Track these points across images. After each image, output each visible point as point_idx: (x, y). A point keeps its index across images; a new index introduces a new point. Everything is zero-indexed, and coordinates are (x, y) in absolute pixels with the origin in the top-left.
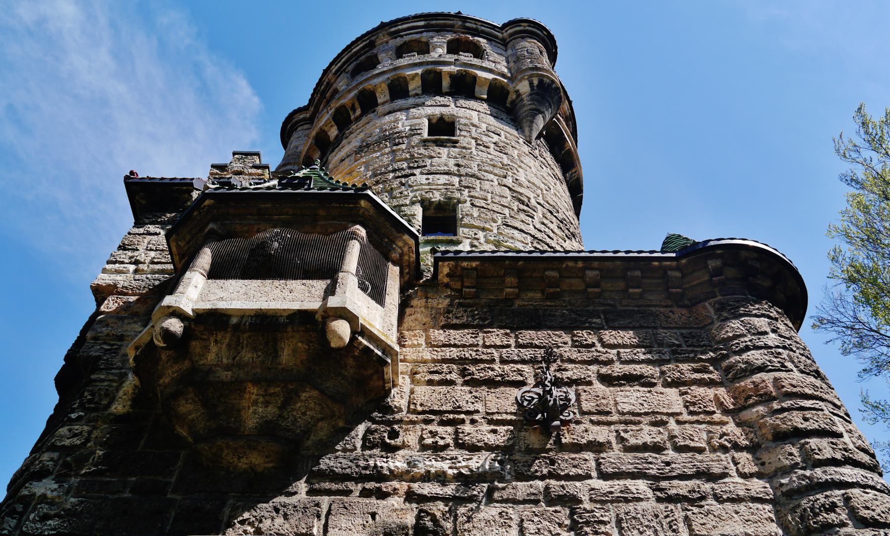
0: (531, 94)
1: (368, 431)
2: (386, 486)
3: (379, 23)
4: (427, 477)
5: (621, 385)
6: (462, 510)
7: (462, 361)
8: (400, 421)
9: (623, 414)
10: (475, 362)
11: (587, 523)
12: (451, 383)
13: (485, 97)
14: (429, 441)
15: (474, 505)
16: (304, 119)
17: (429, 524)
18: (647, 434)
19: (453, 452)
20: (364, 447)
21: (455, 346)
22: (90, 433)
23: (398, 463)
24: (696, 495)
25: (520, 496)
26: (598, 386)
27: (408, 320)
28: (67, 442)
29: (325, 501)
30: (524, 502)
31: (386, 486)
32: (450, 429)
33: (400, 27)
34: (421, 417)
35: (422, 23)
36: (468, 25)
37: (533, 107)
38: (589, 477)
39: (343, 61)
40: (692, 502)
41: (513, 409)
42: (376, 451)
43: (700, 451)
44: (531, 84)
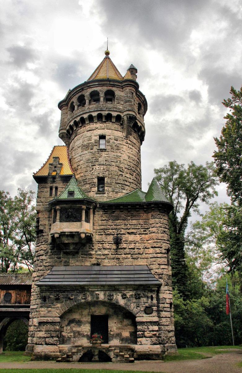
0: (127, 121)
5: (131, 235)
11: (120, 263)
12: (102, 235)
14: (98, 248)
16: (65, 104)
18: (132, 246)
21: (103, 225)
22: (47, 247)
24: (137, 258)
25: (112, 258)
33: (90, 84)
34: (97, 242)
35: (97, 83)
36: (111, 83)
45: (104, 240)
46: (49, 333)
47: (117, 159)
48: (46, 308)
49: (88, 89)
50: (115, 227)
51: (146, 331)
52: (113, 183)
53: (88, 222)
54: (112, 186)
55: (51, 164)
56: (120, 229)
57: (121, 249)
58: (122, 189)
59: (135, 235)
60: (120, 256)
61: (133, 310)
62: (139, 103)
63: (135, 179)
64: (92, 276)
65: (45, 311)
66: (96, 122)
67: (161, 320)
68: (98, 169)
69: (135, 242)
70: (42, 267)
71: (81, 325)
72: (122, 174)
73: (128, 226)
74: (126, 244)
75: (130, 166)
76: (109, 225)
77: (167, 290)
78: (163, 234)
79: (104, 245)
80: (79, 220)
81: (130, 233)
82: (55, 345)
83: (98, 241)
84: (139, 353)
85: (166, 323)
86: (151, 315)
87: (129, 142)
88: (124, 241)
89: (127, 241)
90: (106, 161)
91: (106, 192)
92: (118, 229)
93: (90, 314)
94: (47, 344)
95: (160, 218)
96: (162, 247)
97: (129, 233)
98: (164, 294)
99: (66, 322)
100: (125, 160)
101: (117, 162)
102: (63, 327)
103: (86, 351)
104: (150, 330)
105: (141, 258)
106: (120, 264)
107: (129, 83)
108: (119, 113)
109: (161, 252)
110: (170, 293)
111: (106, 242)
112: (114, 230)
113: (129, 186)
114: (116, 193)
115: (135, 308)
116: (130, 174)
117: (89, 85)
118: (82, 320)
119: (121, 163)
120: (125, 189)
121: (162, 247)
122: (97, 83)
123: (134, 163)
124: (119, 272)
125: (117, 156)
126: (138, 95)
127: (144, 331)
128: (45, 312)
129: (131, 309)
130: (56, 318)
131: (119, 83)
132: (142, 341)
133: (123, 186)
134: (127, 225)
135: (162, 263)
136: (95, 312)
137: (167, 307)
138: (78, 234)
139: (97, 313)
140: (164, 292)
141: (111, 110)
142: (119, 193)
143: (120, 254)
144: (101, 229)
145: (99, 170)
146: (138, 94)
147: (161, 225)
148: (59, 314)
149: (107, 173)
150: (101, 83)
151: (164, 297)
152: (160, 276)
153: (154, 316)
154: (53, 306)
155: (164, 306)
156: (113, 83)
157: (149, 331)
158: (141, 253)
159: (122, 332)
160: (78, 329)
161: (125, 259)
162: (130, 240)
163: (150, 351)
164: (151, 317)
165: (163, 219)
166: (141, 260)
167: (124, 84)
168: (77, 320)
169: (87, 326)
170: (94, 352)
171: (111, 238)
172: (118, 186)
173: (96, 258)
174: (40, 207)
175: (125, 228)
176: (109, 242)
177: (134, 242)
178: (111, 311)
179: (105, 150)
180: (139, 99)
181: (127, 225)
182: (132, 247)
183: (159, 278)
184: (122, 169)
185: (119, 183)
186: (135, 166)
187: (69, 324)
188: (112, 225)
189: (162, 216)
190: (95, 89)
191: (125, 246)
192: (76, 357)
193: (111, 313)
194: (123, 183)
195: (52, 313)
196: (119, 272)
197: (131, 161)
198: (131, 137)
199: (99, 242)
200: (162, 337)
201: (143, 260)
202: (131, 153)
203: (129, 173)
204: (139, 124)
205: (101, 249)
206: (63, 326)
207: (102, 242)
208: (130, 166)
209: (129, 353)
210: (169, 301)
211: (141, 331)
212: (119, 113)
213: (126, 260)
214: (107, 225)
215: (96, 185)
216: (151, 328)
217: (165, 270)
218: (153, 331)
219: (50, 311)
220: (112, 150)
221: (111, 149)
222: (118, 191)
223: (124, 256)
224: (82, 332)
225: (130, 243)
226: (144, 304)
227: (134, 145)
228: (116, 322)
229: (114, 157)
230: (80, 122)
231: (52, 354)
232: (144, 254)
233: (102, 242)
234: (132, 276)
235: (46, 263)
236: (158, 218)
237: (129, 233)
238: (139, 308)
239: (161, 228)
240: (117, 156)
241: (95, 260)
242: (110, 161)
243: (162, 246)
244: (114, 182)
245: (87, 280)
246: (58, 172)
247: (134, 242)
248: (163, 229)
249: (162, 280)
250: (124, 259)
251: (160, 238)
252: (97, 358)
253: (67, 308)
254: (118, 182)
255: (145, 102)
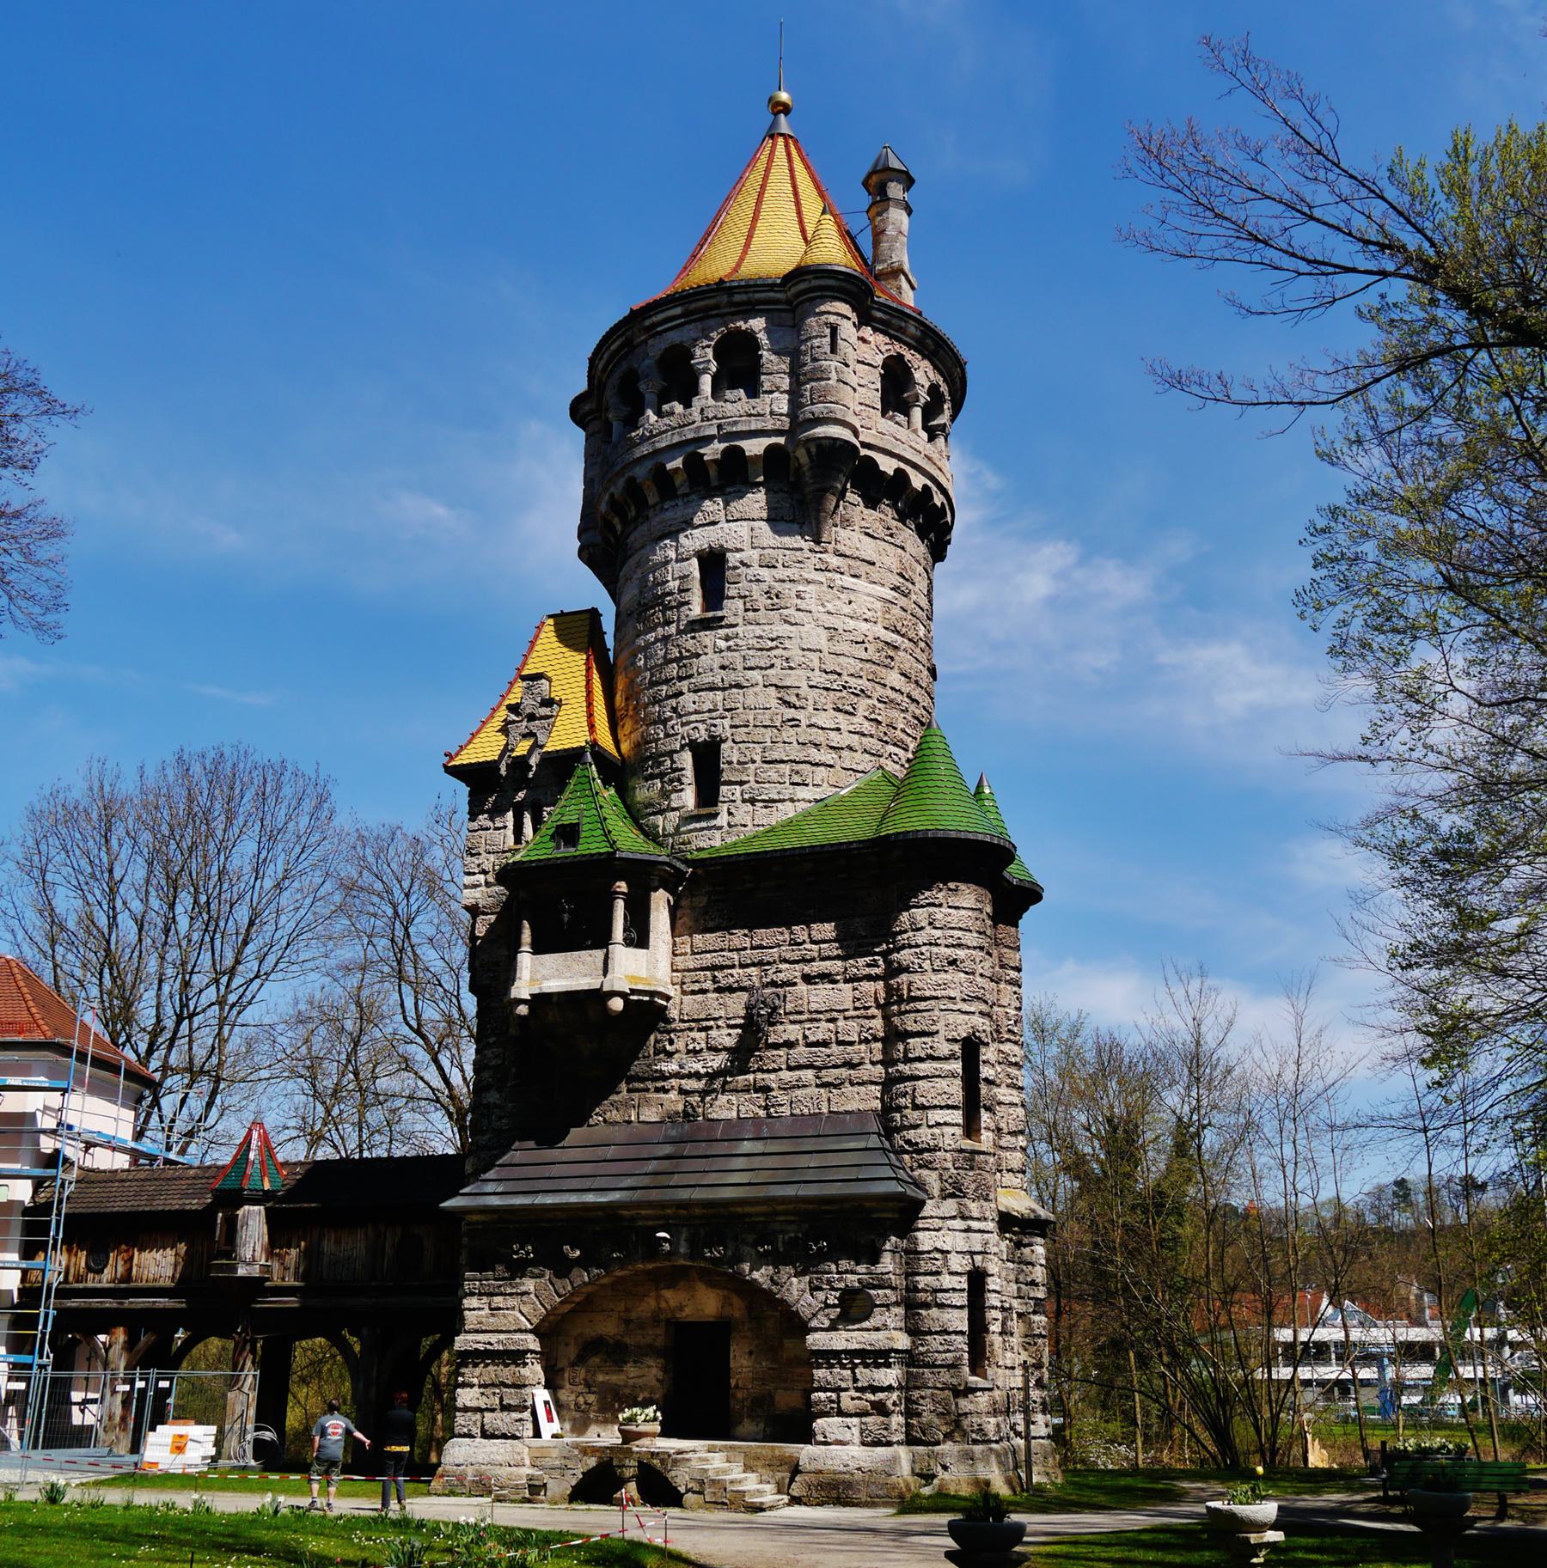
1: (657, 1041)
2: (666, 1084)
3: (627, 312)
4: (690, 1076)
5: (816, 983)
6: (708, 1099)
7: (714, 968)
8: (675, 1030)
9: (811, 1013)
10: (722, 968)
11: (773, 1106)
13: (761, 479)
14: (691, 1047)
15: (714, 1096)
16: (591, 412)
17: (690, 1110)
18: (821, 1031)
19: (706, 1055)
20: (655, 1054)
21: (710, 952)
23: (672, 1067)
25: (740, 1087)
26: (802, 987)
27: (679, 923)
28: (494, 1063)
29: (636, 1096)
30: (742, 1091)
31: (666, 1084)
32: (703, 1034)
33: (654, 319)
34: (687, 1025)
35: (678, 311)
36: (737, 298)
37: (817, 486)
38: (781, 1069)
39: (605, 356)
40: (836, 1086)
41: (742, 1013)
42: (662, 1056)
43: (851, 1043)
44: (809, 452)
45: (712, 1011)
46: (494, 1394)
47: (774, 652)
48: (485, 1299)
49: (650, 342)
50: (756, 955)
51: (846, 1390)
52: (754, 762)
53: (643, 948)
54: (746, 779)
55: (514, 709)
56: (775, 962)
57: (776, 1046)
58: (793, 784)
59: (831, 986)
60: (772, 1076)
61: (798, 1301)
62: (886, 364)
63: (867, 727)
64: (652, 1166)
65: (479, 1309)
66: (687, 495)
67: (922, 1345)
68: (692, 708)
69: (835, 1014)
70: (486, 1137)
71: (625, 1363)
72: (793, 720)
73: (808, 946)
74: (797, 1026)
75: (840, 674)
76: (730, 951)
77: (954, 1218)
78: (943, 975)
79: (713, 1033)
80: (601, 940)
81: (815, 977)
82: (514, 1437)
83: (688, 1021)
84: (813, 1478)
85: (944, 1355)
86: (866, 1324)
87: (835, 561)
88: (791, 1013)
89: (801, 1013)
90: (723, 667)
91: (723, 808)
92: (769, 963)
93: (663, 1317)
94: (485, 1435)
95: (933, 905)
96: (937, 1032)
97: (808, 979)
98: (939, 1234)
99: (572, 1352)
100: (809, 650)
101: (772, 666)
102: (562, 1370)
103: (592, 1462)
104: (860, 1385)
105: (852, 1084)
106: (772, 1110)
107: (815, 283)
108: (774, 440)
109: (929, 1051)
110: (968, 1230)
111: (720, 1023)
112: (749, 970)
113: (831, 766)
114: (766, 807)
115: (807, 1295)
116: (838, 710)
117: (647, 323)
118: (627, 1340)
119: (791, 668)
120: (807, 785)
121: (937, 1032)
122: (678, 311)
123: (864, 655)
124: (758, 1147)
125: (772, 640)
126: (881, 321)
127: (838, 1390)
128: (481, 1313)
129: (790, 1299)
130: (517, 1336)
131: (772, 291)
132: (828, 1430)
133: (797, 772)
134: (804, 942)
135: (936, 1102)
136: (681, 1308)
137: (954, 1290)
138: (598, 997)
139: (688, 1313)
140: (937, 1223)
141: (740, 428)
142: (779, 804)
143: (775, 1071)
144: (702, 969)
145: (697, 712)
146: (879, 315)
147: (938, 933)
148: (528, 1320)
149: (727, 723)
150: (693, 306)
151: (939, 1245)
152: (926, 1155)
153: (877, 1329)
154: (509, 1291)
155: (936, 1285)
156: (744, 297)
157: (857, 1389)
158: (855, 1061)
159: (776, 1389)
160: (615, 1378)
161: (794, 1087)
162: (814, 1007)
163: (859, 1469)
164: (868, 1330)
165: (950, 907)
166: (856, 1089)
167: (794, 290)
168: (611, 1341)
169: (649, 1367)
170: (619, 1467)
171: (736, 1005)
172: (775, 777)
173: (682, 1091)
174: (478, 895)
175: (795, 956)
176: (732, 1022)
177: (828, 1016)
178: (737, 1309)
179: (722, 618)
180: (891, 337)
181: (804, 942)
182: (820, 1036)
183: (920, 1167)
184: (797, 695)
185: (782, 762)
186: (868, 665)
187: (580, 1360)
188: (745, 949)
189: (940, 895)
190: (674, 337)
191: (792, 1032)
192: (560, 1486)
193: (737, 1314)
194: (801, 756)
195: (504, 1316)
196: (758, 1147)
197: (844, 647)
198: (843, 534)
199: (693, 1025)
200: (925, 1414)
201: (862, 1089)
202: (847, 609)
203: (829, 706)
204: (882, 468)
205: (701, 1050)
206: (560, 1365)
207: (704, 1024)
208: (840, 674)
209: (779, 1475)
210: (965, 1262)
211: (825, 1390)
212: (774, 440)
213: (799, 1092)
214: (722, 950)
215: (684, 780)
216: (865, 1375)
217: (948, 1130)
218: (874, 1389)
219: (500, 1309)
220: (750, 614)
221: (746, 610)
222: (776, 797)
223: (786, 1075)
224: (627, 1391)
225: (811, 1020)
226: (840, 1280)
227: (864, 568)
228: (753, 1348)
229: (758, 646)
230: (629, 501)
231: (504, 1472)
232: (869, 1066)
233: (704, 1024)
234: (804, 1161)
235: (501, 1118)
236: (922, 907)
237: (808, 979)
238: (821, 1295)
239: (935, 949)
240: (772, 640)
241: (679, 1097)
242: (740, 667)
243: (934, 1028)
244: (757, 758)
245: (628, 1182)
246: (541, 738)
247: (828, 1016)
248: (943, 950)
249: (935, 1175)
250: (786, 1088)
251: (928, 993)
252: (632, 1489)
253: (559, 1296)
254: (776, 755)
255: (929, 341)
